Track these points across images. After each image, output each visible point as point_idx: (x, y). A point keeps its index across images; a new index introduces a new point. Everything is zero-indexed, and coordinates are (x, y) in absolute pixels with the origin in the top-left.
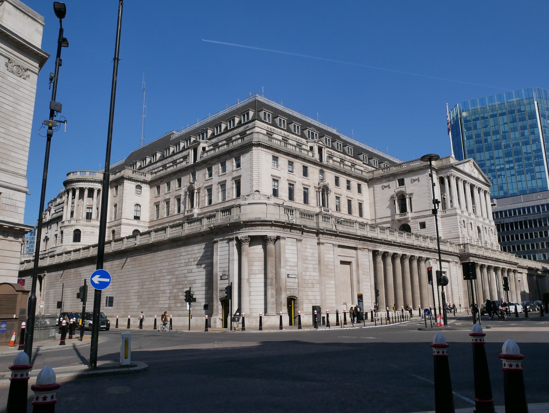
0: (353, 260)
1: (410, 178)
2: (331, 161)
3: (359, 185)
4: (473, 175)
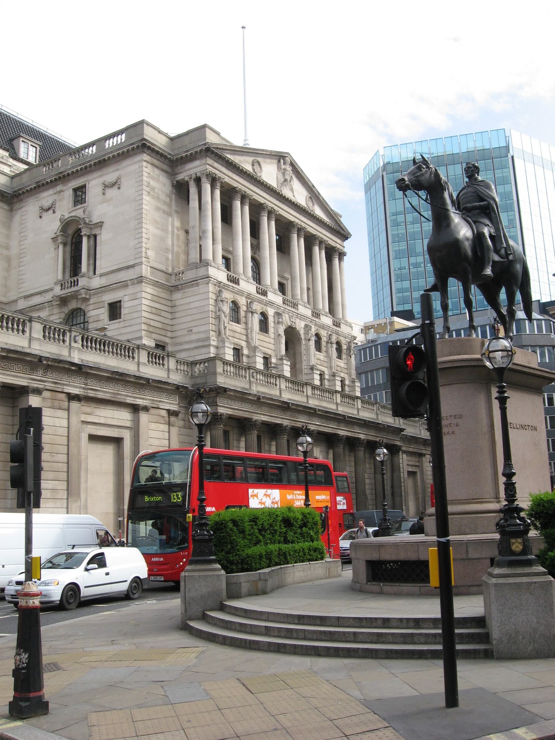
1: (101, 180)
4: (286, 192)
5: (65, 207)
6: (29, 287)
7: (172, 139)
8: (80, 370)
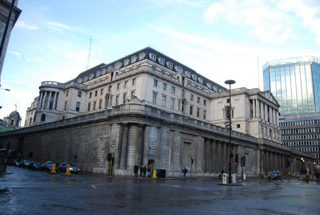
0: (192, 142)
2: (189, 86)
3: (205, 101)
4: (270, 100)
5: (225, 103)
6: (216, 118)
7: (248, 90)
8: (245, 141)
